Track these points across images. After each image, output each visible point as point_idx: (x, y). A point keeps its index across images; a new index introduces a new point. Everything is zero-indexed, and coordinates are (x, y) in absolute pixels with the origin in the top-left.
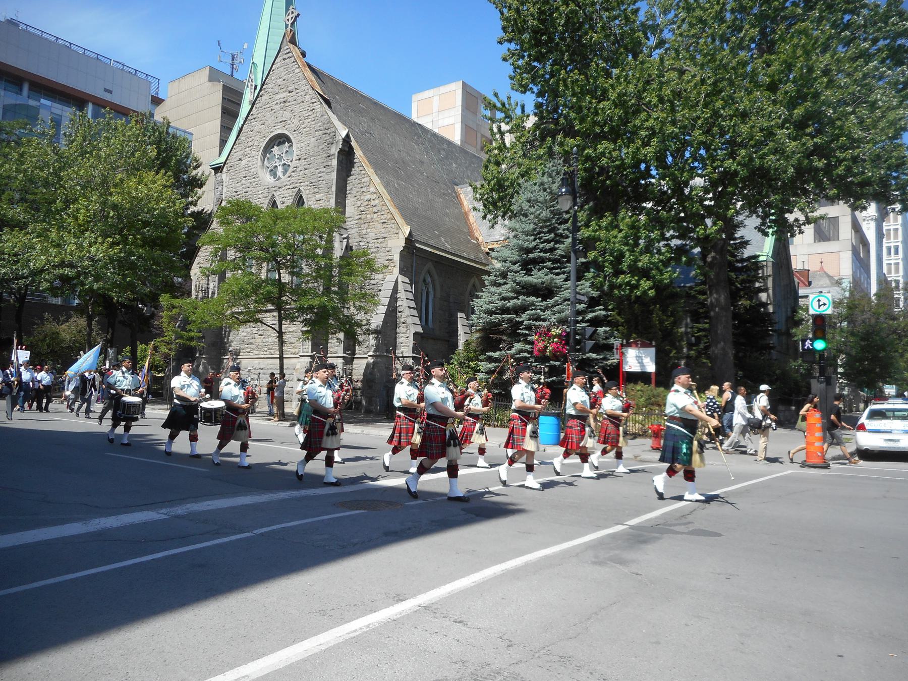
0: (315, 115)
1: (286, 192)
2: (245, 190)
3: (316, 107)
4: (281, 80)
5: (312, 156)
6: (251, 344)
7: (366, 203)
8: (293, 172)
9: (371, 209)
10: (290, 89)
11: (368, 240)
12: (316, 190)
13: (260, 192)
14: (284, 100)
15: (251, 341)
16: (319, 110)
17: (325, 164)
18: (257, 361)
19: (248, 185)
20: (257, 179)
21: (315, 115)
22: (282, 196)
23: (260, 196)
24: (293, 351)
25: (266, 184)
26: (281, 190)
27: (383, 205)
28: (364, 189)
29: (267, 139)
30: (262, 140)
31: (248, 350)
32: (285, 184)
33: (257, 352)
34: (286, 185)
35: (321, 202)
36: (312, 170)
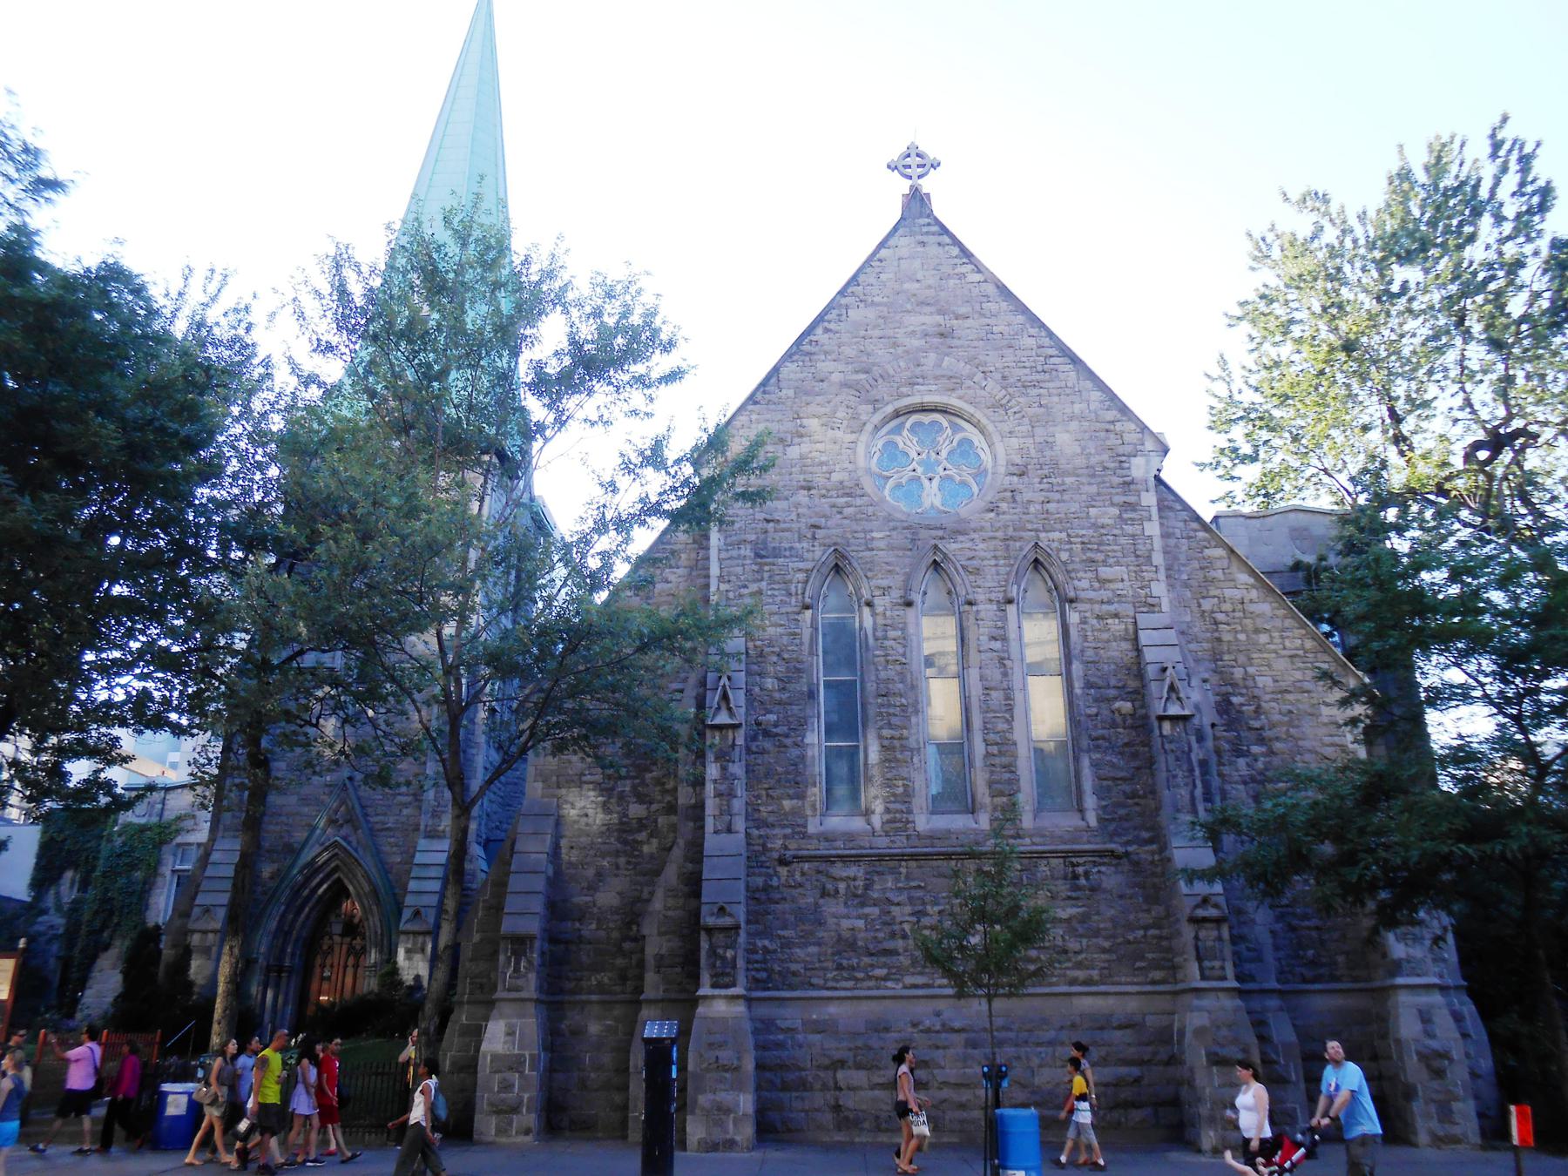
0: (1058, 384)
1: (982, 546)
2: (812, 521)
3: (1061, 368)
4: (917, 285)
5: (1066, 473)
6: (892, 953)
7: (1227, 607)
8: (1003, 500)
9: (1248, 621)
10: (963, 310)
11: (1256, 692)
12: (1100, 557)
13: (875, 535)
14: (942, 329)
15: (889, 945)
16: (1073, 374)
17: (1117, 499)
18: (922, 1009)
19: (828, 511)
20: (859, 501)
21: (1058, 384)
22: (971, 554)
23: (882, 544)
24: (1081, 974)
25: (898, 515)
26: (961, 538)
27: (1285, 617)
28: (1219, 574)
29: (889, 409)
30: (870, 408)
31: (881, 972)
32: (973, 525)
33: (920, 980)
34: (982, 529)
35: (1120, 585)
36: (1074, 507)
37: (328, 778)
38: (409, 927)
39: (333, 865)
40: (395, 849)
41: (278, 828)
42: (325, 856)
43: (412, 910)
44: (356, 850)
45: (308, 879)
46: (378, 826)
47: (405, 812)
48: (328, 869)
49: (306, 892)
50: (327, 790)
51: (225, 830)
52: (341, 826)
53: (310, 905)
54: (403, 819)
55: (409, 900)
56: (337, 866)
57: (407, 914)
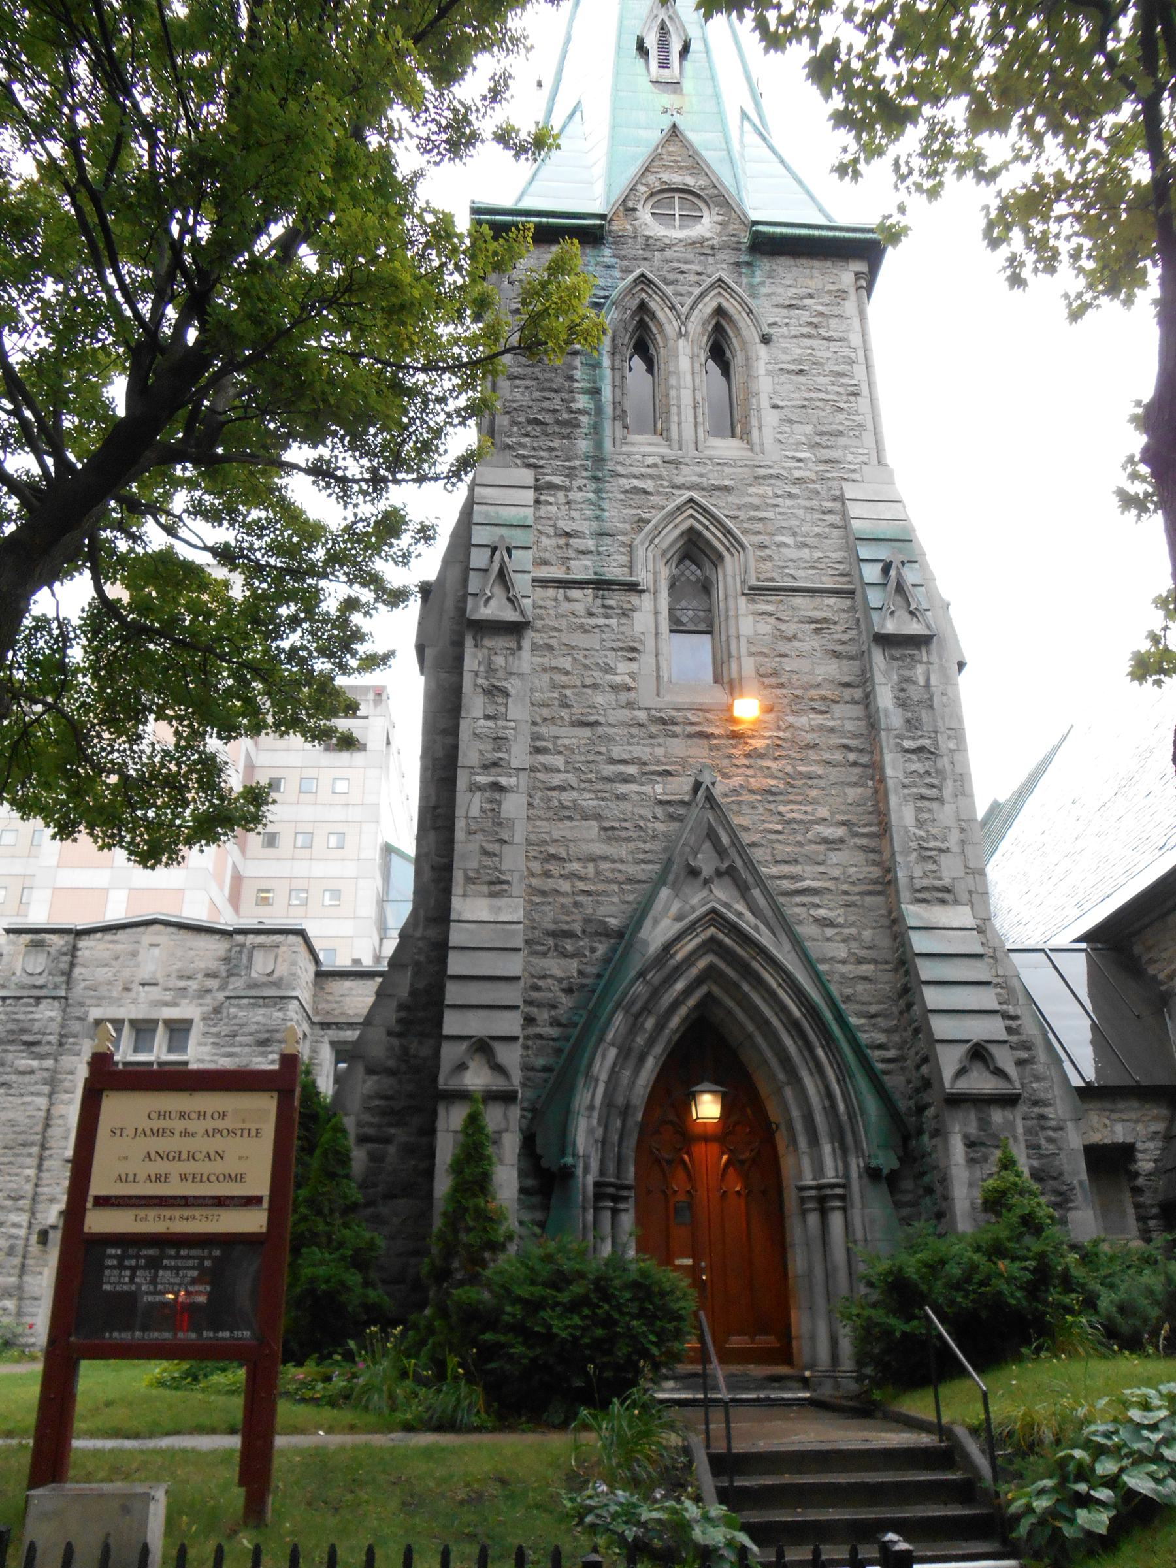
37: (659, 788)
38: (965, 1085)
39: (702, 964)
40: (829, 932)
41: (565, 886)
42: (690, 945)
43: (960, 1051)
44: (756, 929)
45: (656, 993)
46: (786, 885)
47: (834, 857)
48: (694, 972)
49: (650, 1023)
50: (659, 811)
51: (468, 880)
52: (706, 882)
53: (658, 1049)
54: (836, 873)
55: (941, 1027)
56: (711, 967)
57: (949, 1061)
